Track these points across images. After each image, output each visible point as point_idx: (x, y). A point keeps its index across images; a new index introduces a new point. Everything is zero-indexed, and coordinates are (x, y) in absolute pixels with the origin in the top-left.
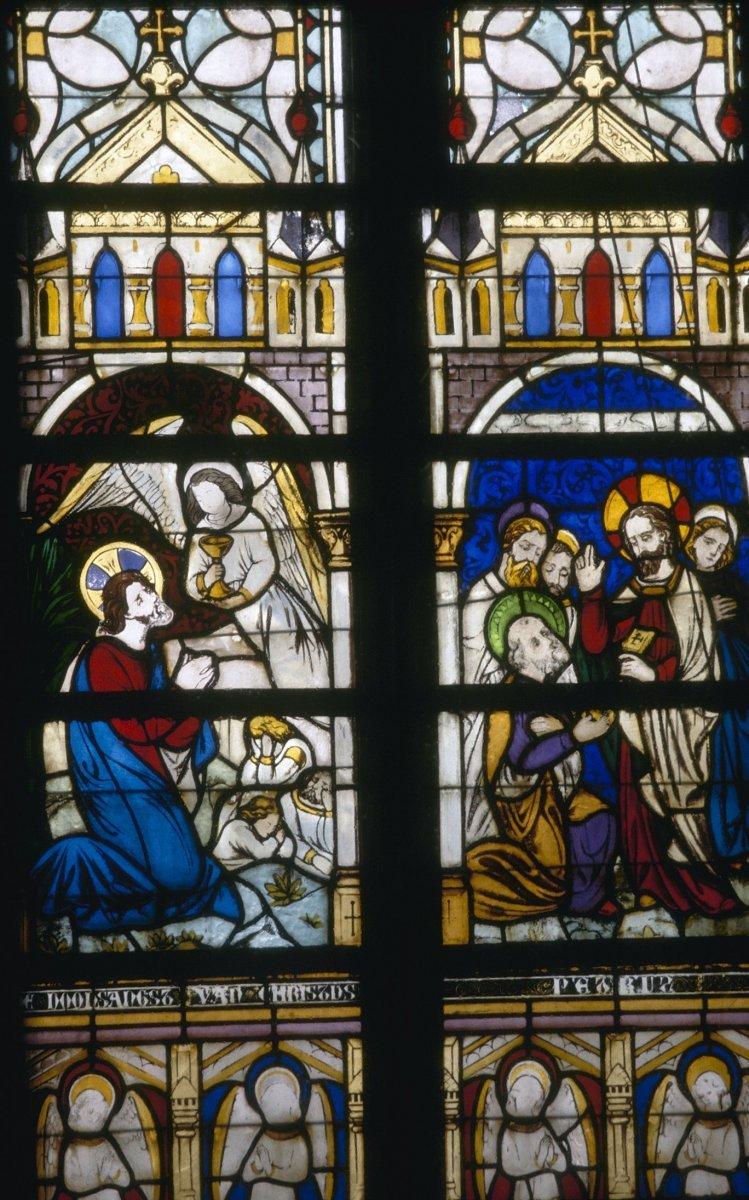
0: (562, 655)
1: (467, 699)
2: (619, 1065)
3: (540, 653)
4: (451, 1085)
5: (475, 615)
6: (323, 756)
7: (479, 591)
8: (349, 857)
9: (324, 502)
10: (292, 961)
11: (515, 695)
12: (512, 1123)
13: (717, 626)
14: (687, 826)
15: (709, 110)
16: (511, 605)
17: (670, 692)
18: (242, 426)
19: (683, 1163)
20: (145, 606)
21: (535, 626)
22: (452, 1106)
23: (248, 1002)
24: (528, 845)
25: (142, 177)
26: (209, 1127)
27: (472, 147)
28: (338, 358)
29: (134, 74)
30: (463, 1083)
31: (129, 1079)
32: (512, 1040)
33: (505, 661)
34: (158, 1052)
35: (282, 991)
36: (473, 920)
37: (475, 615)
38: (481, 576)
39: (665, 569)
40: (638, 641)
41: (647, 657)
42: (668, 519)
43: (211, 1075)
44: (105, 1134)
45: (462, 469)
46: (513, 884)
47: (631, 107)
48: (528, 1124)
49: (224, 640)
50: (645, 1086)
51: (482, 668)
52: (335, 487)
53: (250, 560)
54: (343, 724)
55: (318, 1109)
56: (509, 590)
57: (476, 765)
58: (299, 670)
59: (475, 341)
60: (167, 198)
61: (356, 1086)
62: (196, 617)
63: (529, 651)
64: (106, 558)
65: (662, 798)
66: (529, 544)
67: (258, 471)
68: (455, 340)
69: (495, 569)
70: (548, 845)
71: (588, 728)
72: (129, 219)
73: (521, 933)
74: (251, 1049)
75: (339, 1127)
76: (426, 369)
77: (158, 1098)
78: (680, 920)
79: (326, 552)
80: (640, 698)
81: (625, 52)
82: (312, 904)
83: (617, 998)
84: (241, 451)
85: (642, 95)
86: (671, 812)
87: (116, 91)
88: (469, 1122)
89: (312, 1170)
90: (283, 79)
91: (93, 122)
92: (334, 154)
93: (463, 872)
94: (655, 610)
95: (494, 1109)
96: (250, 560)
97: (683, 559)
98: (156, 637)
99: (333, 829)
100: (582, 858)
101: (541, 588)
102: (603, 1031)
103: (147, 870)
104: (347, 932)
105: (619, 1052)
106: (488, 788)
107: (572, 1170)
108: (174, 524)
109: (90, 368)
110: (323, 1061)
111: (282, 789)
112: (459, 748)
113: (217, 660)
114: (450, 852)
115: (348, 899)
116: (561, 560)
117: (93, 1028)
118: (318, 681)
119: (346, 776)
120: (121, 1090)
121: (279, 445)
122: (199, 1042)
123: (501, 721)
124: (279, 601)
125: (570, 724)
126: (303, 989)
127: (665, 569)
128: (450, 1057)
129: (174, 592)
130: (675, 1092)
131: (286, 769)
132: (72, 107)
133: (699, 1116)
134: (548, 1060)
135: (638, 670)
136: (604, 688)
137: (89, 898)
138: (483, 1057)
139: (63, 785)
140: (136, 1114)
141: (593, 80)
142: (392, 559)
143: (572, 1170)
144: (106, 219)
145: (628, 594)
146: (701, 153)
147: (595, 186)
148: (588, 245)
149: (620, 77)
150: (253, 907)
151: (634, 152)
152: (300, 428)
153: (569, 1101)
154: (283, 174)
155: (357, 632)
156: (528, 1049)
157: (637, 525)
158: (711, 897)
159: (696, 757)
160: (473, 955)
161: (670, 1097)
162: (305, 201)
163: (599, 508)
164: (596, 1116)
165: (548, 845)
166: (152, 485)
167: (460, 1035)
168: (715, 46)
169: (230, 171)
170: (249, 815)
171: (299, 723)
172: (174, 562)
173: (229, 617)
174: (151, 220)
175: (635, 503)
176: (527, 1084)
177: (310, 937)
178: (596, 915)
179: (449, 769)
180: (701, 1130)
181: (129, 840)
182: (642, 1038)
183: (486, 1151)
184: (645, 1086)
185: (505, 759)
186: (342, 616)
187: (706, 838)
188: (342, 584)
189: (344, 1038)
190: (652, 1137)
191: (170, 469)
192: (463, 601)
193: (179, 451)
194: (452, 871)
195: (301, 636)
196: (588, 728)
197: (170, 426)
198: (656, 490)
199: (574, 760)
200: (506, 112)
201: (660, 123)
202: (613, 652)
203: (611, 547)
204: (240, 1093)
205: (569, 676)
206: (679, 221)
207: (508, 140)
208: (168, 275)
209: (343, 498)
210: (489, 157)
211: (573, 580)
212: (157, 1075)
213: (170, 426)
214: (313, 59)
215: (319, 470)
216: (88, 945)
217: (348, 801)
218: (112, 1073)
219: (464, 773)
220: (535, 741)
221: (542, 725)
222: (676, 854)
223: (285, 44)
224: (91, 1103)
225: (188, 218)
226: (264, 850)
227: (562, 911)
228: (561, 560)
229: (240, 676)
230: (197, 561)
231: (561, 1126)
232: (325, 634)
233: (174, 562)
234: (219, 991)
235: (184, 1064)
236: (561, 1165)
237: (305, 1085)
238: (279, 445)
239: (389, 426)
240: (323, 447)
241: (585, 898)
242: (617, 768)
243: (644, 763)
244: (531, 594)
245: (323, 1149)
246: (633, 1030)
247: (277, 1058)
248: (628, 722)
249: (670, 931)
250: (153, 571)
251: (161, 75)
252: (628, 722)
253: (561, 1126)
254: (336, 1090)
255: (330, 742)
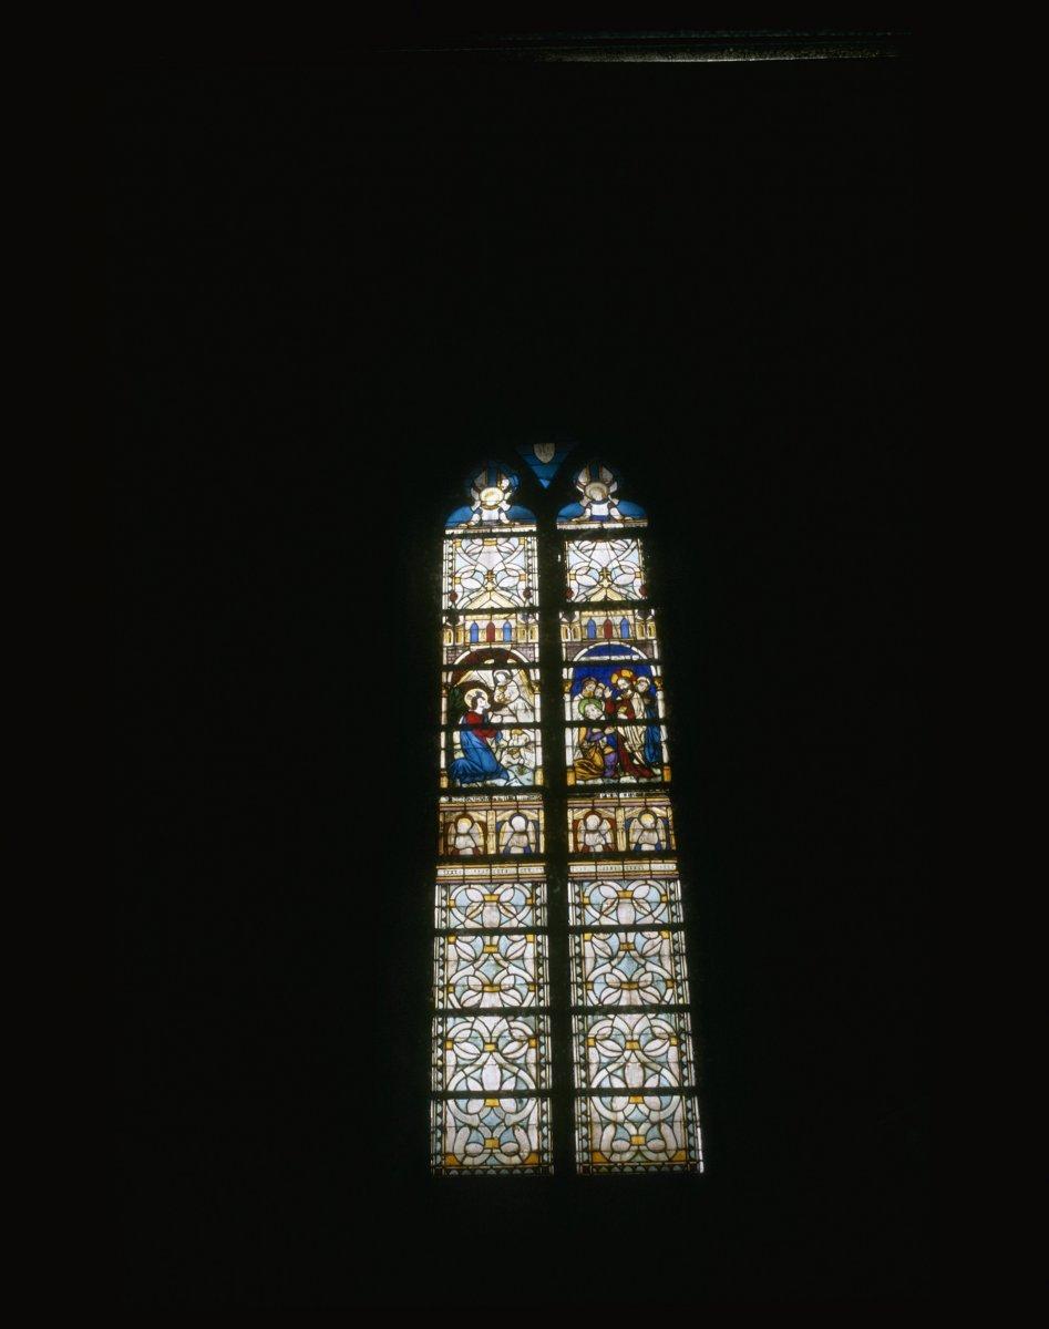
0: (600, 713)
1: (573, 724)
2: (620, 816)
3: (594, 712)
4: (570, 821)
5: (575, 705)
6: (532, 739)
7: (576, 698)
8: (540, 763)
9: (533, 678)
10: (524, 790)
11: (587, 723)
12: (587, 831)
13: (645, 705)
14: (638, 755)
15: (637, 590)
16: (586, 702)
17: (632, 721)
18: (510, 661)
19: (640, 842)
20: (483, 704)
21: (593, 706)
22: (570, 827)
23: (510, 800)
24: (592, 760)
25: (485, 607)
26: (498, 832)
27: (573, 598)
28: (537, 646)
29: (483, 586)
30: (574, 821)
31: (475, 819)
32: (589, 810)
33: (584, 715)
34: (484, 813)
35: (519, 797)
36: (576, 779)
37: (575, 705)
38: (577, 694)
39: (630, 692)
40: (623, 709)
41: (625, 713)
42: (629, 680)
43: (499, 819)
44: (468, 834)
45: (571, 670)
46: (587, 769)
47: (616, 589)
48: (593, 832)
49: (505, 711)
50: (628, 821)
51: (578, 717)
52: (536, 675)
53: (512, 691)
54: (538, 731)
55: (531, 827)
56: (585, 698)
57: (576, 741)
58: (525, 718)
59: (575, 640)
60: (492, 611)
61: (542, 821)
62: (496, 707)
63: (592, 713)
64: (472, 692)
65: (630, 748)
66: (590, 687)
67: (514, 671)
68: (569, 640)
69: (581, 692)
70: (598, 760)
71: (608, 731)
72: (480, 616)
73: (590, 782)
74: (511, 812)
75: (537, 832)
76: (561, 647)
77: (484, 825)
78: (637, 779)
79: (533, 691)
80: (623, 724)
81: (613, 577)
82: (529, 775)
83: (619, 799)
84: (510, 667)
85: (617, 586)
86: (634, 752)
87: (478, 590)
88: (575, 831)
89: (529, 844)
90: (522, 586)
91: (472, 596)
92: (535, 599)
93: (573, 767)
94: (627, 702)
95: (583, 828)
96: (512, 691)
97: (634, 689)
98: (486, 711)
99: (535, 758)
100: (608, 764)
101: (594, 697)
102: (615, 807)
103: (482, 767)
104: (539, 781)
105: (620, 812)
106: (580, 746)
107: (607, 844)
108: (491, 684)
109: (469, 649)
110: (532, 815)
111: (519, 747)
112: (571, 737)
113: (502, 716)
114: (569, 762)
115: (539, 774)
116: (600, 691)
117: (465, 807)
118: (531, 720)
119: (539, 743)
120: (473, 822)
121: (520, 665)
122: (496, 810)
123: (583, 730)
124: (520, 701)
125: (603, 731)
126: (526, 797)
127: (630, 692)
128: (570, 813)
129: (491, 700)
130: (637, 823)
131: (522, 742)
132: (466, 594)
133: (645, 829)
134: (599, 815)
135: (622, 716)
136: (612, 720)
137: (465, 775)
138: (579, 814)
139: (459, 747)
140: (478, 829)
141: (606, 583)
142: (552, 693)
143: (607, 844)
144: (474, 617)
145: (619, 698)
146: (635, 598)
147: (607, 605)
148: (605, 618)
149: (612, 582)
150: (512, 776)
151: (617, 598)
152: (526, 661)
153: (606, 825)
154: (522, 605)
155: (542, 709)
156: (593, 811)
157: (621, 682)
158: (646, 772)
159: (640, 737)
160: (575, 787)
161: (635, 824)
162: (531, 610)
163: (610, 679)
164: (614, 829)
165: (598, 760)
166: (486, 676)
167: (573, 808)
168: (638, 575)
169: (506, 605)
170: (511, 753)
171: (526, 731)
172: (490, 692)
173: (506, 706)
174: (486, 616)
175: (620, 676)
176: (593, 821)
177: (527, 783)
178: (612, 777)
179: (568, 741)
180: (646, 833)
181: (476, 759)
182: (627, 809)
183: (580, 838)
184: (628, 821)
185: (585, 738)
186: (538, 705)
187: (644, 758)
188: (538, 698)
189: (539, 809)
190: (631, 835)
191: (491, 672)
192: (572, 701)
193: (493, 667)
194: (570, 767)
195: (526, 710)
196: (608, 731)
197: (491, 662)
198: (626, 673)
199: (605, 739)
200: (582, 591)
201: (622, 591)
202: (616, 712)
203: (614, 688)
204: (507, 823)
205: (603, 718)
206: (630, 612)
207: (583, 596)
208: (491, 630)
209: (538, 677)
210: (578, 600)
211: (603, 695)
212: (483, 818)
213: (491, 662)
214: (530, 581)
215: (531, 671)
216: (464, 786)
217: (539, 750)
218: (470, 818)
219: (573, 742)
220: (593, 734)
221: (595, 730)
222: (635, 762)
223: (523, 577)
224: (464, 825)
225: (496, 616)
226: (515, 762)
227: (602, 777)
228: (600, 691)
229: (509, 720)
230: (497, 692)
231: (603, 832)
232: (533, 709)
233: (490, 692)
234: (502, 797)
235: (491, 816)
236: (604, 842)
237: (527, 821)
238: (520, 665)
239: (551, 658)
240: (533, 665)
241: (608, 774)
242: (617, 742)
243: (626, 739)
244: (592, 698)
245: (532, 838)
246: (624, 807)
247: (519, 814)
248: (620, 730)
249: (635, 781)
250: (485, 695)
251: (490, 586)
252: (620, 730)
253: (603, 832)
254: (536, 823)
255: (536, 736)
